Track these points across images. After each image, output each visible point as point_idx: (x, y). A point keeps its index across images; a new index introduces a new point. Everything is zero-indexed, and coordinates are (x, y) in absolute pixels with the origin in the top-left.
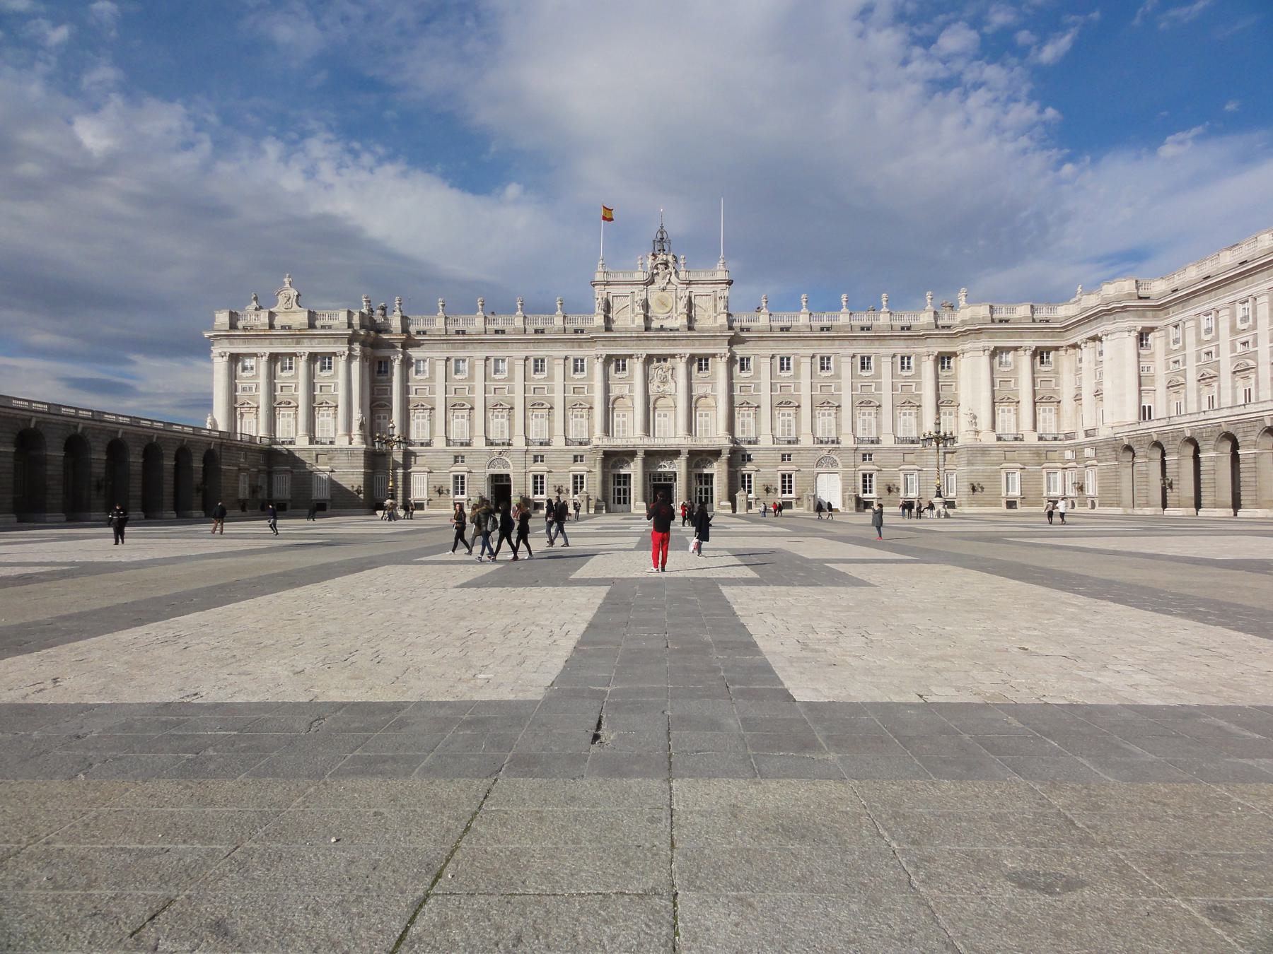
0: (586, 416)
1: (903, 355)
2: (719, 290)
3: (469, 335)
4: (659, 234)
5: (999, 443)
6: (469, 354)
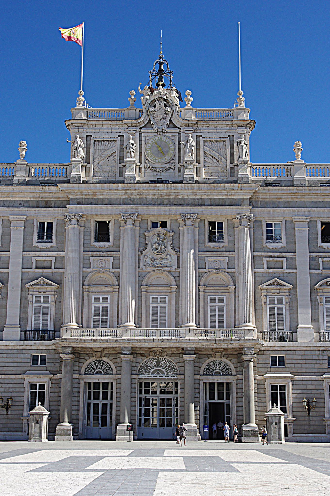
0: (52, 299)
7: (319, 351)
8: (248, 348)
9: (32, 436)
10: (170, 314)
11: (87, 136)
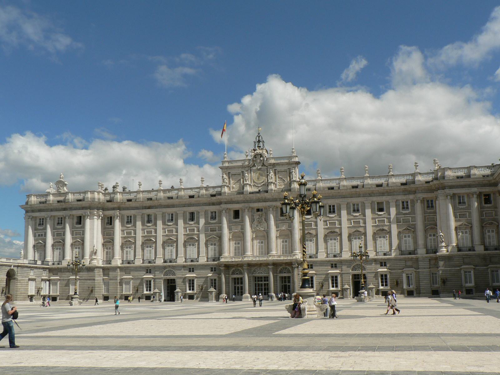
0: (217, 244)
1: (403, 200)
2: (291, 168)
4: (258, 138)
5: (459, 253)
7: (327, 261)
8: (294, 262)
9: (209, 300)
10: (265, 248)
11: (229, 173)
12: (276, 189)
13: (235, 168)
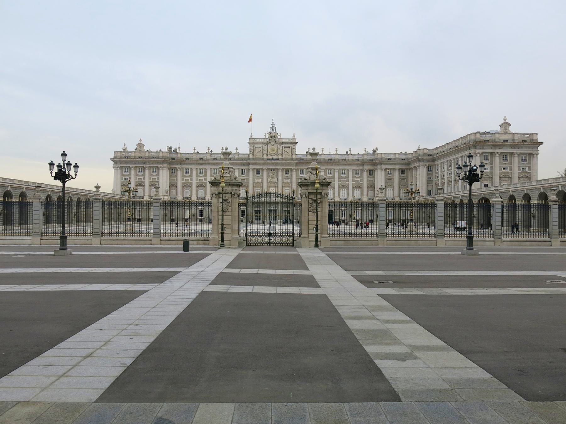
2: (293, 146)
3: (205, 160)
4: (272, 126)
6: (204, 167)
12: (283, 158)
13: (258, 143)
